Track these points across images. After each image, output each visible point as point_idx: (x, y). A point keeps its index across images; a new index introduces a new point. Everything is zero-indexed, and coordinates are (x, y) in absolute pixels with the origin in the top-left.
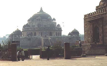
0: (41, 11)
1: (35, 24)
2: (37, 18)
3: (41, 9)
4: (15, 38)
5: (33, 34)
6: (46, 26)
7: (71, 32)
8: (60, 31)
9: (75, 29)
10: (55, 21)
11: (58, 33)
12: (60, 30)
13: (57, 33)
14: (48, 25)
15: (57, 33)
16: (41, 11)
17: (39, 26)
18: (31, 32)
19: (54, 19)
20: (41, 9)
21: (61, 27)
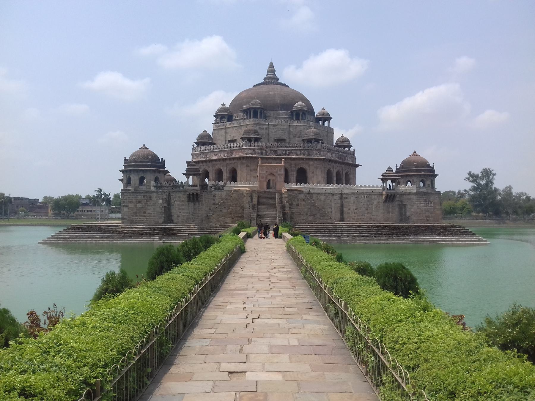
0: (272, 78)
2: (245, 107)
3: (272, 70)
4: (129, 188)
5: (225, 175)
6: (283, 140)
7: (394, 170)
8: (349, 165)
9: (415, 154)
10: (326, 124)
11: (338, 174)
13: (334, 174)
14: (291, 136)
15: (334, 174)
16: (272, 78)
17: (250, 140)
20: (272, 70)
21: (352, 149)
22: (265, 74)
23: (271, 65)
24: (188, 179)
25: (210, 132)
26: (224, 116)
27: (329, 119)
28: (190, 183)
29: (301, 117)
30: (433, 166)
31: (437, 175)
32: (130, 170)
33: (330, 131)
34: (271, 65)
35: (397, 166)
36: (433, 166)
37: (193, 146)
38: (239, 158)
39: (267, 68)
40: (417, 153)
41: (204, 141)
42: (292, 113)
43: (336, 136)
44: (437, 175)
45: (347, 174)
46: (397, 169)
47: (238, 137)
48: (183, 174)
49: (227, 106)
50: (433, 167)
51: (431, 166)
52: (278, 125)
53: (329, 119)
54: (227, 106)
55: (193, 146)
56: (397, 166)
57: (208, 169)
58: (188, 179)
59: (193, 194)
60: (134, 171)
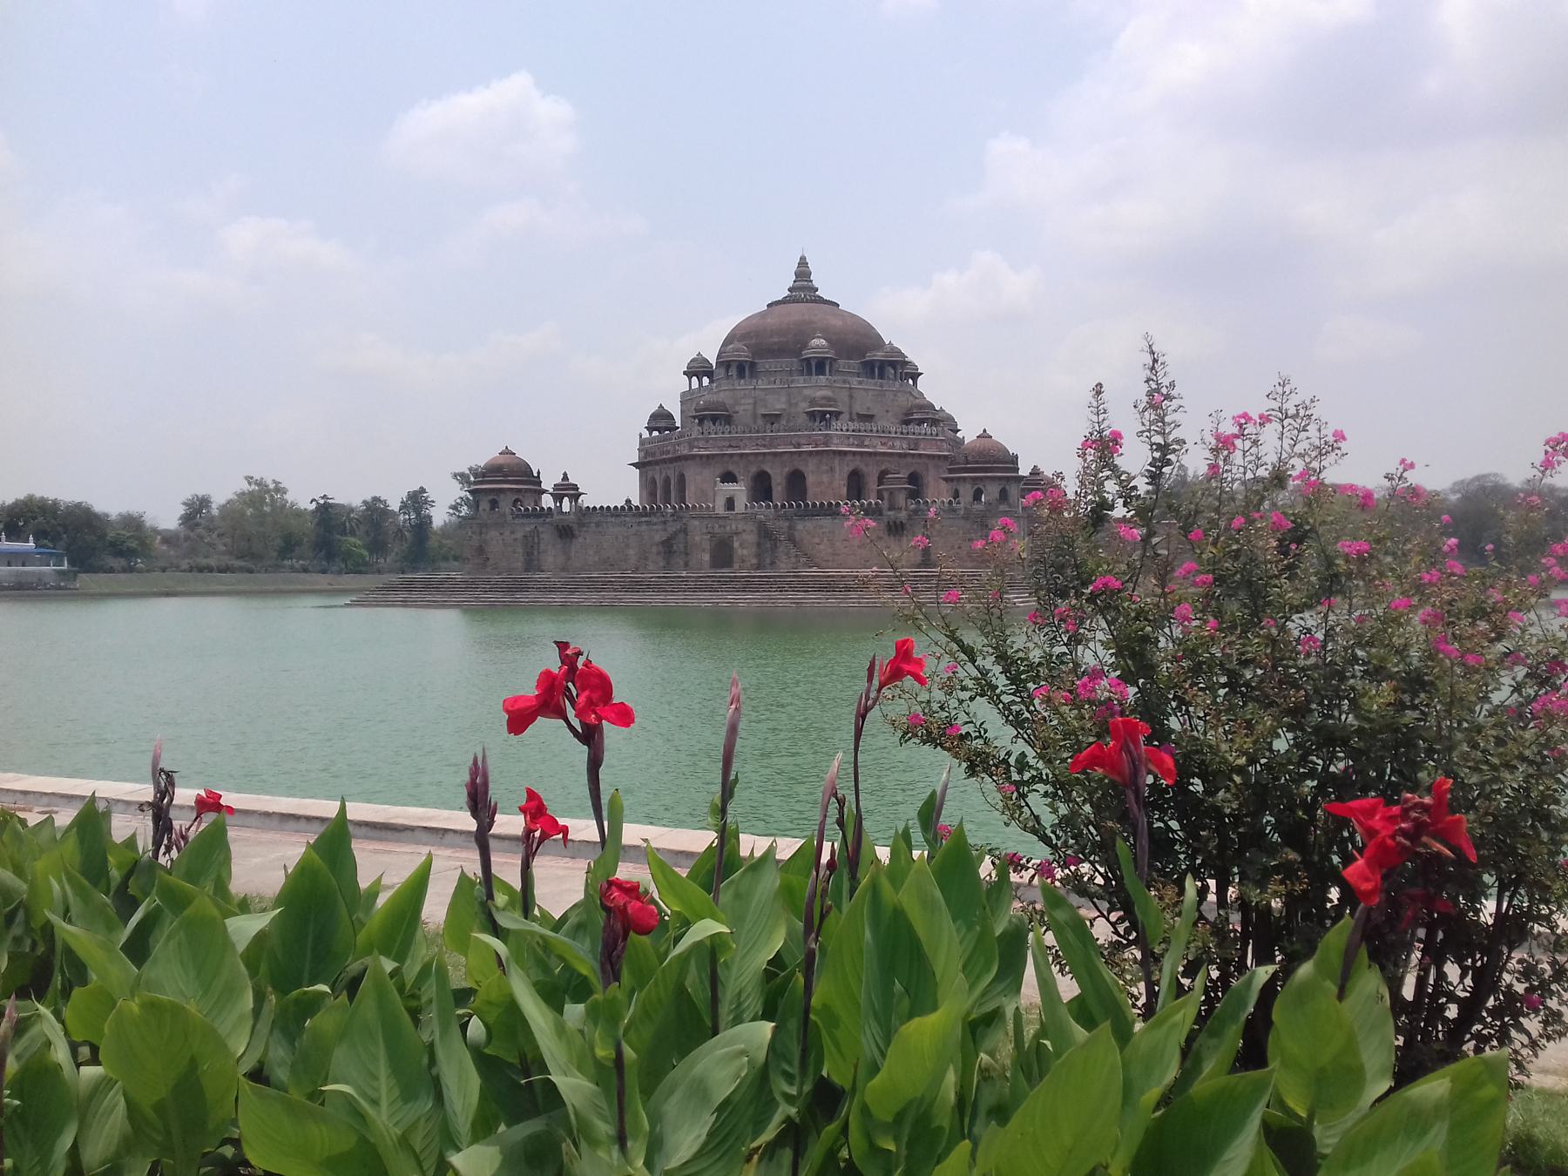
3: (803, 272)
20: (803, 272)
23: (803, 262)
34: (803, 262)
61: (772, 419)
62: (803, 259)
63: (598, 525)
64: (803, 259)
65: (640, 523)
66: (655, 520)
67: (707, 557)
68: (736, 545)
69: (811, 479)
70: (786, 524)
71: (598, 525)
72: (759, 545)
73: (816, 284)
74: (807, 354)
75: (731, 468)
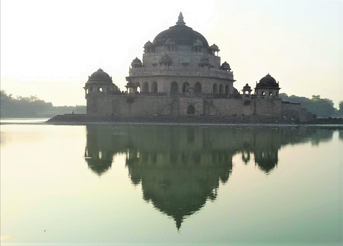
1: (157, 58)
3: (181, 17)
11: (221, 86)
12: (230, 78)
13: (218, 87)
18: (144, 81)
19: (215, 48)
20: (181, 17)
21: (231, 71)
22: (177, 20)
24: (127, 89)
25: (141, 58)
26: (149, 48)
27: (218, 50)
28: (129, 92)
29: (198, 51)
30: (278, 82)
31: (280, 89)
32: (93, 84)
33: (218, 59)
35: (257, 82)
36: (278, 82)
37: (130, 67)
38: (159, 76)
39: (178, 15)
40: (270, 74)
41: (136, 63)
42: (193, 47)
43: (222, 63)
44: (280, 89)
45: (227, 87)
46: (257, 84)
47: (157, 62)
48: (125, 86)
49: (152, 41)
50: (278, 84)
51: (277, 82)
52: (183, 55)
53: (218, 50)
54: (152, 41)
55: (130, 67)
56: (257, 82)
57: (139, 82)
58: (127, 89)
59: (130, 98)
60: (95, 84)
61: (185, 64)
62: (181, 13)
63: (142, 98)
64: (181, 13)
65: (158, 98)
66: (164, 97)
67: (186, 110)
68: (196, 106)
69: (203, 86)
70: (210, 100)
71: (142, 98)
72: (204, 107)
73: (185, 22)
74: (195, 45)
75: (176, 81)
